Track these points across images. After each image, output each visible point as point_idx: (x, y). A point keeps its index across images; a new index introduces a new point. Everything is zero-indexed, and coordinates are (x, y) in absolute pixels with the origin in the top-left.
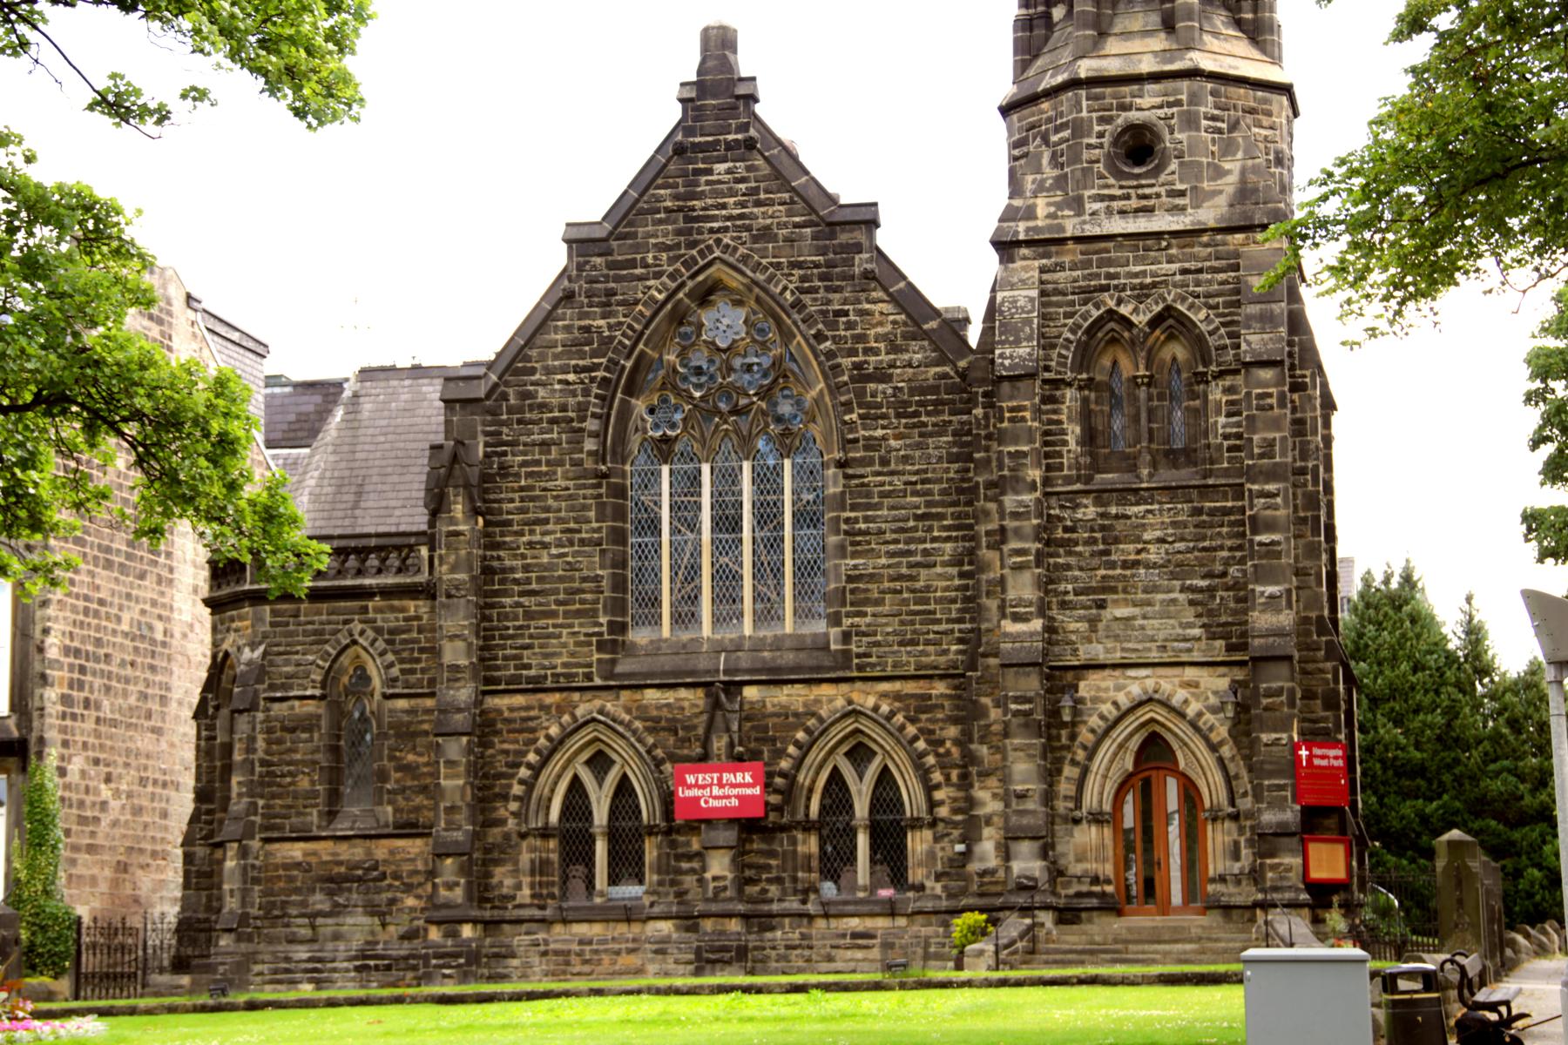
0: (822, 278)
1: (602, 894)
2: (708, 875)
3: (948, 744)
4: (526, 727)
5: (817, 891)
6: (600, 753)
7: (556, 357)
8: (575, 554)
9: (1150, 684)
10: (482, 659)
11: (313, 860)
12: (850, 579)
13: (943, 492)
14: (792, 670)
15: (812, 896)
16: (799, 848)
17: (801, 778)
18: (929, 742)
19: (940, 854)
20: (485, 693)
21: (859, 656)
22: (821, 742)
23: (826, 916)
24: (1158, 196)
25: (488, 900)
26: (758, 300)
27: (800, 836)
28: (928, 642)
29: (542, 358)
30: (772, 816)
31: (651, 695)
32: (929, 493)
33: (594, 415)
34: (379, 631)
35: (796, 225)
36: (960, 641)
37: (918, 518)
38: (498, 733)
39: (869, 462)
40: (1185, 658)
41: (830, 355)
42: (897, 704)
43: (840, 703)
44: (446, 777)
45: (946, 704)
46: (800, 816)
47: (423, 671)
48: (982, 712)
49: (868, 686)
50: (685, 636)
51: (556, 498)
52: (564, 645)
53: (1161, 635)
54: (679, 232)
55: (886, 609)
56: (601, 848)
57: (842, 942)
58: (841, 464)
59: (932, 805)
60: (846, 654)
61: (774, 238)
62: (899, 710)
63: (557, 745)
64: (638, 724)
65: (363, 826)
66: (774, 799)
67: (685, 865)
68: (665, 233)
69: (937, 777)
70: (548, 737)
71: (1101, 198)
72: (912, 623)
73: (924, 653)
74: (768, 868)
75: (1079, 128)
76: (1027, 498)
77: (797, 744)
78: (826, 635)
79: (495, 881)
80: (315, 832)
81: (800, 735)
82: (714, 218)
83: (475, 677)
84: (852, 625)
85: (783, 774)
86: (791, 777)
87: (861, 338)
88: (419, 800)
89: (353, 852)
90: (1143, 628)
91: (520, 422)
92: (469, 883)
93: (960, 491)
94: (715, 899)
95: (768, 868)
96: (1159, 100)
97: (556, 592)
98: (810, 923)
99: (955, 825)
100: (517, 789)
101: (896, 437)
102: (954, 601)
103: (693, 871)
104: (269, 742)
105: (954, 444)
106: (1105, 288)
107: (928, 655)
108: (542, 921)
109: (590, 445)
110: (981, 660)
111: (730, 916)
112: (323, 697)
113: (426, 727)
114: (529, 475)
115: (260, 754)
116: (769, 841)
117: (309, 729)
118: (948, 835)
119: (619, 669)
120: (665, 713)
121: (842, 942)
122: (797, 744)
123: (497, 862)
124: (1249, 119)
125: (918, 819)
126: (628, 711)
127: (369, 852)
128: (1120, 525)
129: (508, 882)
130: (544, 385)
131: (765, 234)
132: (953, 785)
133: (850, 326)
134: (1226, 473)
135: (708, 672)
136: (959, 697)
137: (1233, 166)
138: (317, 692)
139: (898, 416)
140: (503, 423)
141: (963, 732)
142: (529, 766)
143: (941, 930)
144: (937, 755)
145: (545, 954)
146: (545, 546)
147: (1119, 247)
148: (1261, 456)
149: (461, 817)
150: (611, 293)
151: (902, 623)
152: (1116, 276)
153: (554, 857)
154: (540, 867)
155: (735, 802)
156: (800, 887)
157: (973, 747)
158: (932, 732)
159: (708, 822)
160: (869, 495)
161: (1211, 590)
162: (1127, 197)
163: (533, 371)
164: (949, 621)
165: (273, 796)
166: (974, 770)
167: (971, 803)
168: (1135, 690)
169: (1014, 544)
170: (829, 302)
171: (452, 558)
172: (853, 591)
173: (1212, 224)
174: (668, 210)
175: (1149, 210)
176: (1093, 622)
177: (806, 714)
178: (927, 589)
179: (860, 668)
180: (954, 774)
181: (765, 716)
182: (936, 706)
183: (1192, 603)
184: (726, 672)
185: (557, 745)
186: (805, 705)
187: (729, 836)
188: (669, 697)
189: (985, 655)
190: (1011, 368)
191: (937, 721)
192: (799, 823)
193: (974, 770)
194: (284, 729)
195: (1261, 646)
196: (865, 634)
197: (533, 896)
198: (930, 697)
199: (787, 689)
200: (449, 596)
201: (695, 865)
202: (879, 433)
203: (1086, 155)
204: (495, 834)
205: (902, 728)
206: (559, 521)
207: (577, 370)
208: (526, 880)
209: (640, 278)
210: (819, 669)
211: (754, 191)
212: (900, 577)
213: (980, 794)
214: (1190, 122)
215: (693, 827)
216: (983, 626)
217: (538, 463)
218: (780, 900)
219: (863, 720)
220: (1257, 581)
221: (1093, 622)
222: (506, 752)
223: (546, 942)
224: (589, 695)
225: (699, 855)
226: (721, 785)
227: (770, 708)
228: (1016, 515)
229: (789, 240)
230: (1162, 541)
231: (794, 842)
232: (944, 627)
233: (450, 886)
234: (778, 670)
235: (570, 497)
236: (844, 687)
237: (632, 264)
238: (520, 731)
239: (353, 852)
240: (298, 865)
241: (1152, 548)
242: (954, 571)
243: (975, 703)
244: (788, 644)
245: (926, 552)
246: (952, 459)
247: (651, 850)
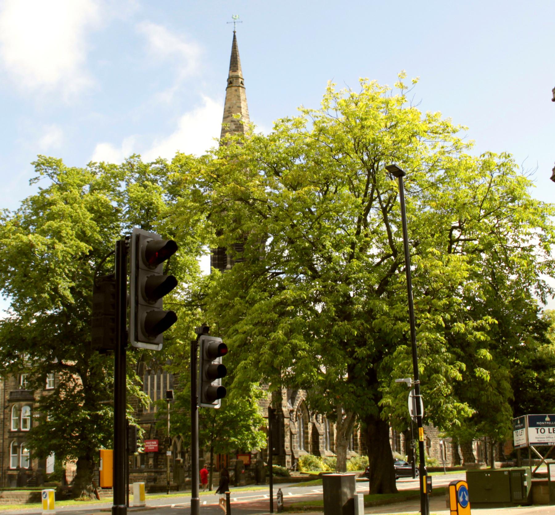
74: (161, 462)
94: (150, 468)
111: (152, 472)
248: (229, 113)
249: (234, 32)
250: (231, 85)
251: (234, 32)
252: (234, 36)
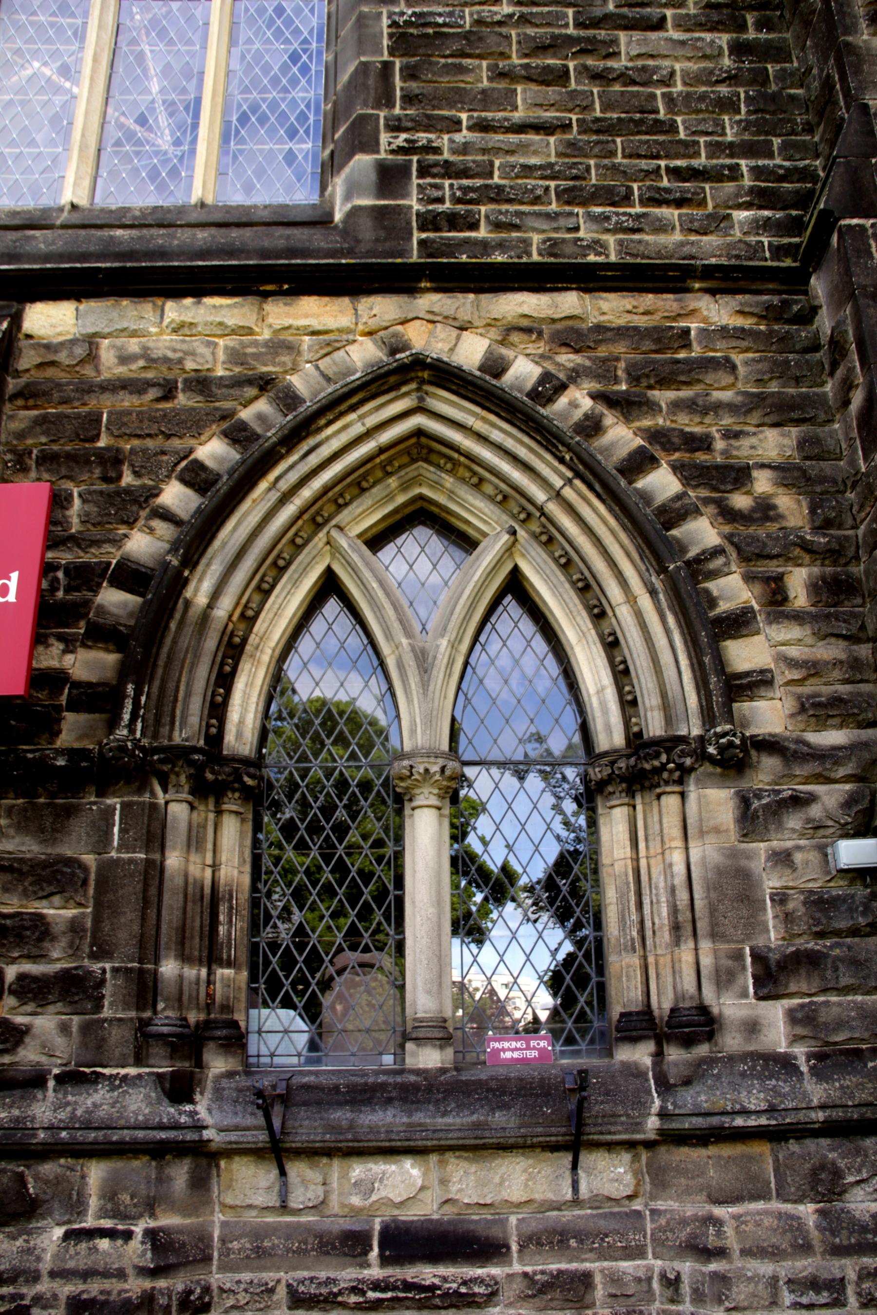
3: (763, 483)
5: (235, 1040)
15: (218, 1064)
16: (173, 860)
17: (199, 591)
19: (771, 882)
22: (287, 470)
23: (277, 1152)
27: (178, 812)
28: (656, 199)
30: (73, 730)
36: (761, 198)
42: (567, 359)
45: (738, 359)
46: (188, 729)
49: (463, 304)
57: (348, 1275)
62: (575, 376)
66: (88, 664)
69: (733, 590)
77: (197, 477)
81: (212, 450)
84: (409, 149)
85: (129, 576)
86: (160, 588)
98: (200, 1183)
102: (729, 105)
107: (663, 227)
116: (52, 822)
118: (798, 802)
121: (348, 1275)
122: (197, 477)
125: (671, 743)
132: (798, 617)
143: (807, 1211)
144: (728, 514)
151: (572, 148)
156: (164, 1019)
158: (703, 443)
177: (238, 382)
180: (798, 581)
181: (88, 388)
182: (708, 364)
186: (236, 356)
191: (717, 407)
192: (182, 753)
196: (449, 170)
199: (176, 310)
205: (592, 427)
218: (71, 1079)
219: (445, 402)
227: (109, 364)
231: (153, 832)
236: (382, 308)
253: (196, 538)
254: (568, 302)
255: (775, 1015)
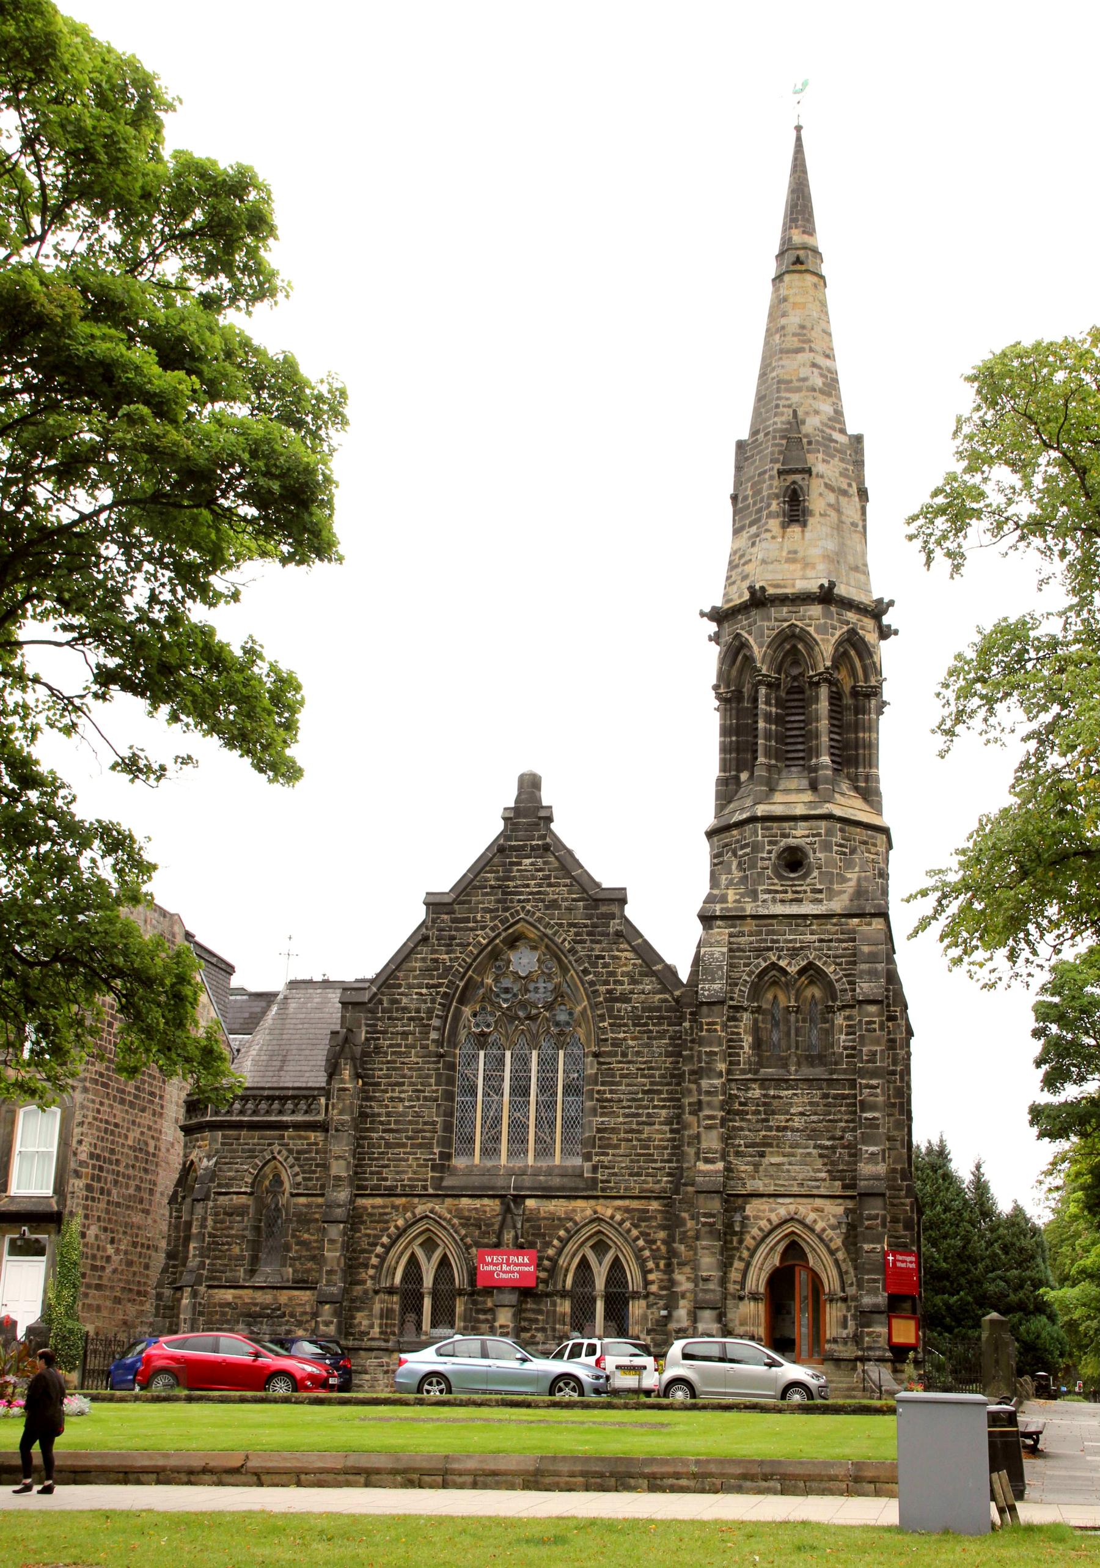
0: (589, 934)
1: (426, 1334)
2: (497, 1324)
4: (382, 1220)
6: (429, 1239)
7: (415, 978)
8: (420, 1106)
9: (792, 1208)
10: (356, 1173)
11: (239, 1301)
12: (599, 1131)
13: (662, 1076)
14: (558, 1189)
17: (561, 1262)
18: (646, 1241)
20: (357, 1195)
21: (602, 1182)
24: (805, 892)
25: (352, 1334)
26: (547, 947)
29: (406, 978)
31: (465, 1201)
32: (653, 1076)
33: (438, 1016)
34: (290, 1151)
35: (574, 900)
36: (669, 1175)
37: (645, 1092)
38: (363, 1222)
39: (616, 1055)
40: (815, 1192)
41: (592, 983)
43: (589, 1212)
44: (329, 1250)
46: (559, 1287)
47: (317, 1179)
48: (682, 1223)
49: (608, 1202)
50: (489, 1164)
51: (410, 1069)
52: (410, 1166)
53: (800, 1176)
54: (498, 901)
55: (622, 1151)
56: (427, 1303)
58: (596, 1055)
59: (647, 1283)
60: (594, 1180)
61: (559, 908)
63: (402, 1232)
64: (455, 1221)
65: (274, 1280)
66: (543, 1275)
67: (482, 1317)
68: (490, 902)
69: (650, 1264)
70: (397, 1227)
71: (769, 892)
72: (638, 1161)
73: (645, 1182)
74: (536, 1321)
75: (756, 847)
76: (716, 1082)
77: (560, 1239)
78: (582, 1167)
79: (356, 1321)
80: (241, 1283)
81: (562, 1233)
82: (521, 893)
83: (351, 1185)
85: (549, 1259)
86: (554, 1261)
87: (612, 974)
88: (310, 1265)
89: (265, 1298)
90: (788, 1171)
91: (389, 1018)
92: (339, 1323)
93: (673, 1076)
95: (536, 1321)
96: (807, 832)
97: (407, 1131)
99: (661, 1297)
100: (374, 1261)
101: (633, 1039)
102: (666, 1148)
103: (487, 1321)
104: (215, 1222)
105: (670, 1045)
106: (770, 949)
108: (386, 1350)
109: (434, 1035)
110: (682, 1188)
112: (251, 1194)
113: (317, 1216)
114: (393, 1053)
115: (209, 1229)
117: (242, 1215)
119: (445, 1183)
120: (474, 1214)
122: (560, 1239)
123: (359, 1309)
124: (863, 847)
126: (450, 1212)
127: (275, 1298)
128: (775, 1102)
129: (365, 1322)
130: (406, 995)
131: (554, 905)
133: (605, 965)
134: (845, 1071)
135: (503, 1188)
136: (667, 1212)
137: (852, 876)
138: (248, 1190)
139: (635, 1025)
140: (378, 1019)
141: (669, 1236)
142: (383, 1245)
144: (651, 1250)
145: (387, 1372)
146: (401, 1100)
147: (780, 924)
148: (868, 1061)
149: (337, 1278)
150: (453, 938)
151: (632, 1161)
152: (777, 941)
153: (397, 1307)
154: (387, 1314)
155: (517, 1275)
157: (675, 1245)
158: (649, 1234)
159: (498, 1288)
160: (614, 1076)
161: (833, 1147)
162: (786, 892)
163: (400, 986)
164: (662, 1161)
165: (216, 1258)
166: (675, 1261)
167: (672, 1283)
168: (783, 1212)
169: (707, 1112)
170: (592, 950)
171: (340, 1106)
172: (600, 1139)
173: (839, 911)
174: (492, 887)
175: (800, 901)
176: (756, 1166)
178: (649, 1139)
179: (603, 1190)
180: (662, 1263)
181: (539, 1219)
182: (651, 1218)
183: (821, 1156)
184: (515, 1189)
185: (402, 1232)
187: (512, 1298)
188: (478, 1203)
189: (685, 1185)
190: (709, 997)
193: (675, 1261)
194: (225, 1213)
195: (866, 1187)
196: (607, 1168)
197: (381, 1333)
198: (648, 1211)
199: (554, 1202)
200: (337, 1130)
201: (489, 1317)
202: (622, 1035)
203: (760, 864)
204: (358, 1290)
205: (629, 1231)
206: (411, 1084)
207: (428, 986)
208: (377, 1322)
209: (472, 929)
210: (576, 1189)
211: (548, 877)
212: (632, 1131)
213: (679, 1277)
214: (827, 847)
215: (488, 1291)
216: (685, 1165)
217: (400, 1046)
220: (864, 1143)
221: (756, 1166)
222: (368, 1235)
223: (388, 1365)
224: (424, 1200)
225: (491, 1311)
226: (508, 1264)
228: (708, 1093)
229: (567, 909)
230: (802, 1114)
231: (554, 1304)
232: (659, 1165)
233: (327, 1324)
234: (550, 1189)
235: (420, 1069)
236: (592, 1202)
237: (467, 920)
238: (378, 1222)
239: (265, 1298)
240: (229, 1304)
241: (796, 1119)
242: (667, 1128)
243: (678, 1216)
244: (556, 1171)
245: (649, 1115)
246: (669, 1054)
247: (460, 1306)
248: (804, 342)
249: (798, 129)
250: (799, 267)
251: (798, 129)
252: (799, 139)
253: (560, 1252)
254: (627, 1202)
255: (649, 1338)
